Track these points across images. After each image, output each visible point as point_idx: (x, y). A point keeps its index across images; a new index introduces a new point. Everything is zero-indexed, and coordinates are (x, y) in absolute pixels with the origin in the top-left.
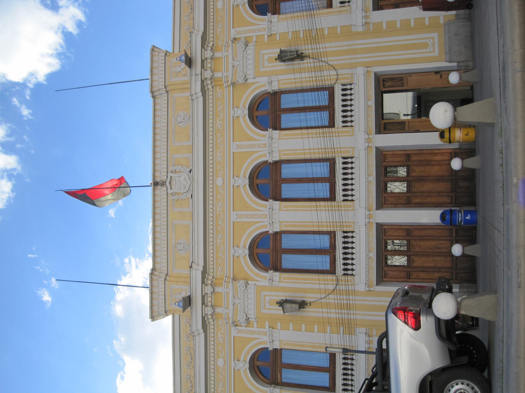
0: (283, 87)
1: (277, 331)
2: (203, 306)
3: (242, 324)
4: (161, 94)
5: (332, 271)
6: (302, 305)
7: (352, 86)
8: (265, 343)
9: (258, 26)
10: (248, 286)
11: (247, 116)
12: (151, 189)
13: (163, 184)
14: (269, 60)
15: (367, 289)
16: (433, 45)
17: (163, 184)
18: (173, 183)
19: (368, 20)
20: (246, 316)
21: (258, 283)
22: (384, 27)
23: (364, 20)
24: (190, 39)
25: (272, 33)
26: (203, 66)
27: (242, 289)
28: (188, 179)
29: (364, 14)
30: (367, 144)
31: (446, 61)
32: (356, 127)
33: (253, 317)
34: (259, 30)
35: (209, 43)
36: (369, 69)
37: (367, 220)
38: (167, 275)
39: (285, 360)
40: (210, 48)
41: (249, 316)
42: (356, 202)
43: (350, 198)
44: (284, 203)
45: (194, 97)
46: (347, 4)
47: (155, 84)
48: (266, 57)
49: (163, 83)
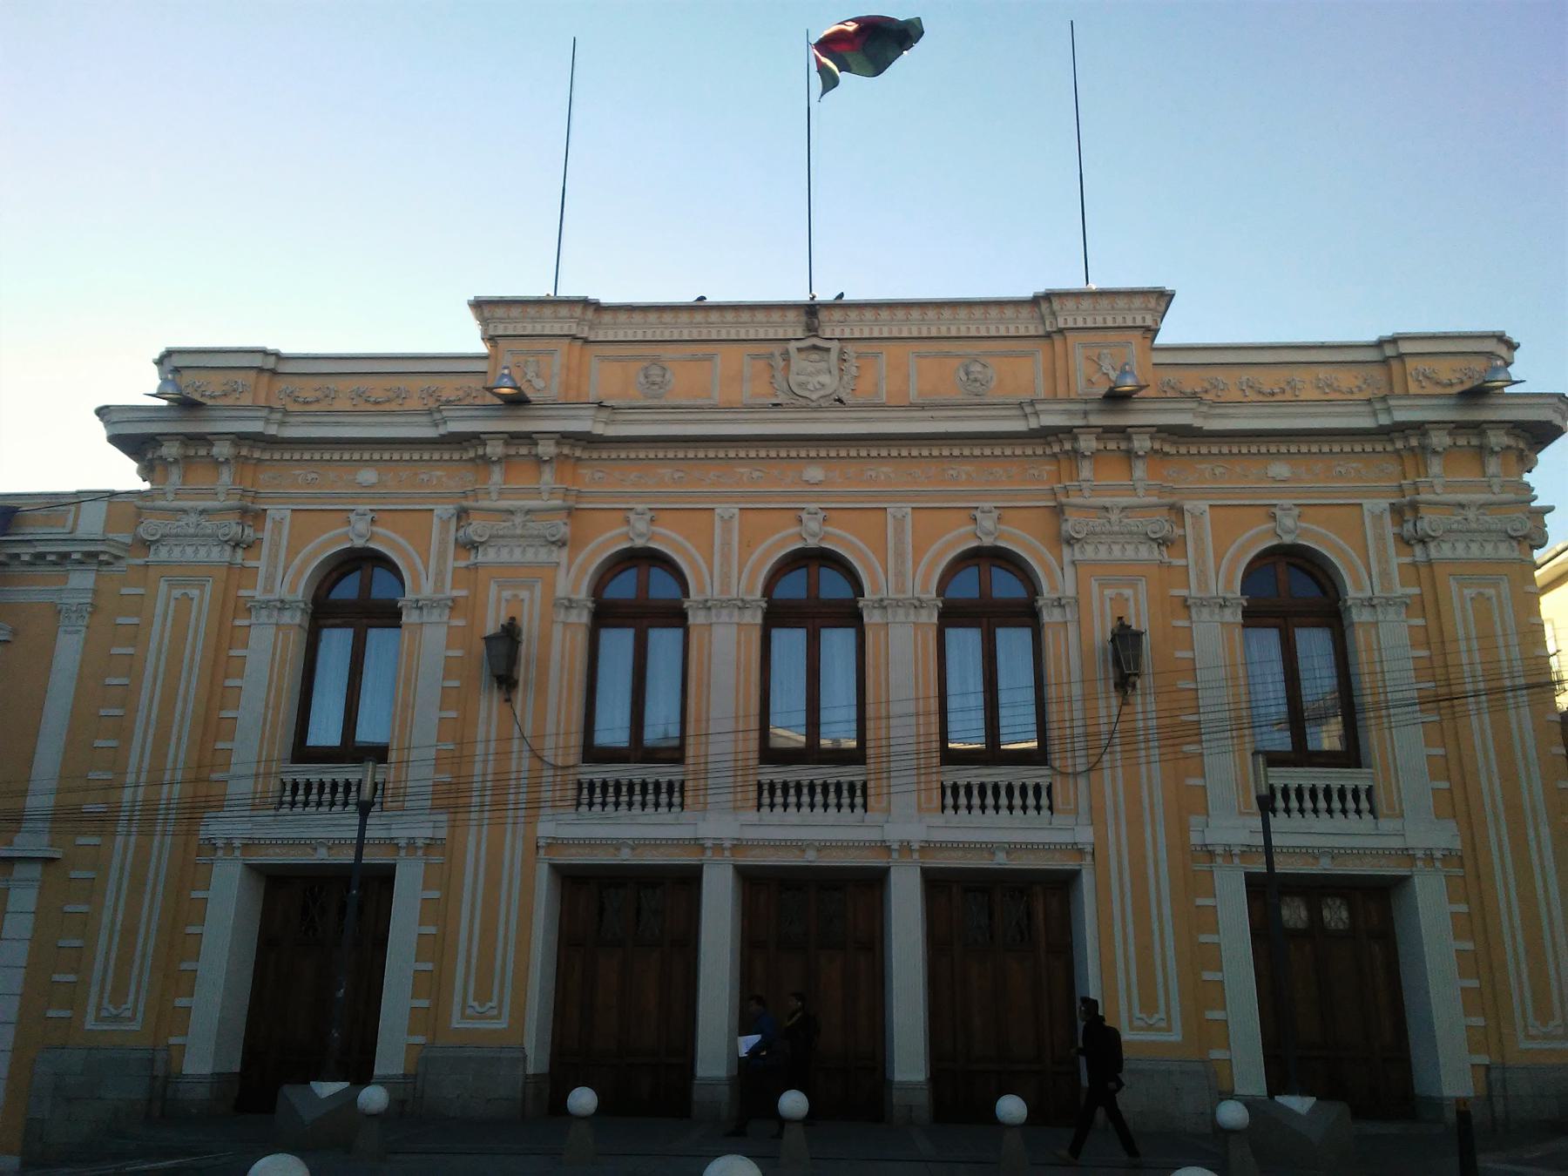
0: (1049, 637)
1: (445, 618)
3: (461, 533)
4: (1042, 318)
5: (593, 754)
6: (506, 681)
7: (1045, 812)
8: (417, 587)
9: (1213, 575)
10: (554, 548)
11: (974, 544)
12: (803, 297)
13: (812, 330)
14: (1119, 600)
15: (542, 843)
16: (1150, 1028)
17: (812, 330)
18: (814, 356)
19: (1219, 860)
21: (562, 572)
22: (1200, 902)
23: (1219, 850)
24: (1189, 390)
25: (1194, 611)
26: (1108, 430)
27: (547, 533)
28: (822, 393)
29: (1236, 850)
30: (895, 846)
32: (938, 819)
33: (480, 558)
34: (1202, 574)
35: (1174, 443)
36: (1089, 858)
37: (709, 844)
38: (586, 341)
39: (374, 635)
40: (1157, 446)
42: (752, 816)
43: (766, 800)
44: (756, 635)
45: (1028, 410)
47: (1070, 304)
48: (1128, 592)
49: (1070, 324)
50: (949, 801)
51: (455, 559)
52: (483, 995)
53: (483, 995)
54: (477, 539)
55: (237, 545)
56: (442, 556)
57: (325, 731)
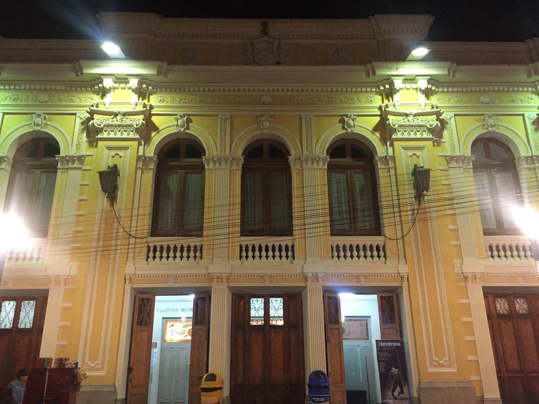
16: (440, 366)
31: (420, 382)
43: (244, 254)
46: (490, 253)
50: (336, 254)
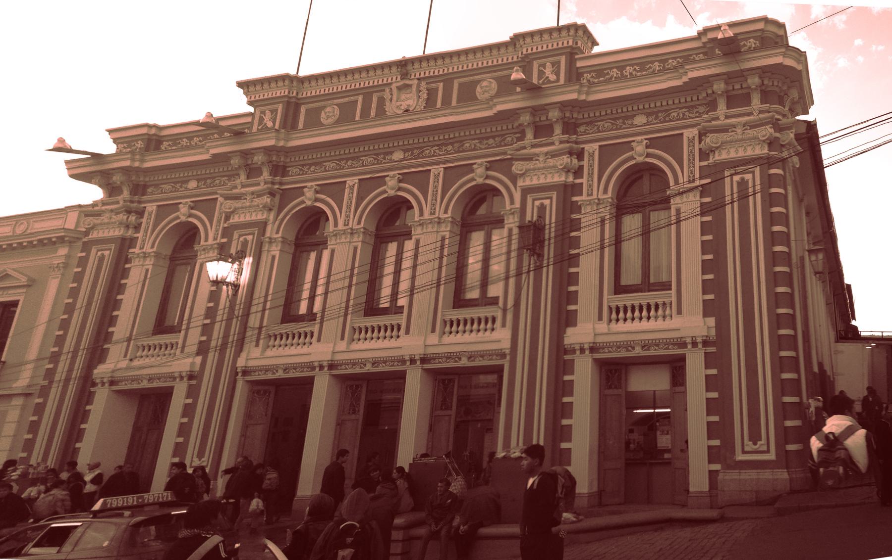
1: (698, 198)
2: (725, 76)
20: (717, 148)
41: (716, 153)
51: (700, 161)
52: (755, 437)
53: (755, 437)
54: (714, 145)
55: (569, 171)
56: (691, 161)
57: (632, 276)
